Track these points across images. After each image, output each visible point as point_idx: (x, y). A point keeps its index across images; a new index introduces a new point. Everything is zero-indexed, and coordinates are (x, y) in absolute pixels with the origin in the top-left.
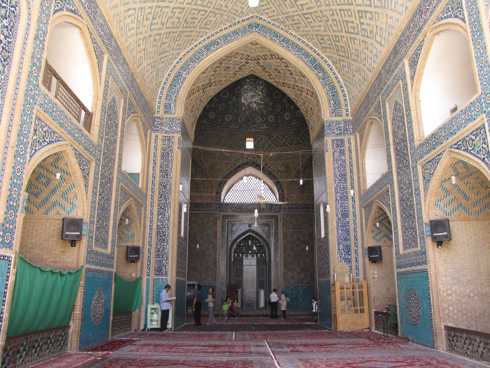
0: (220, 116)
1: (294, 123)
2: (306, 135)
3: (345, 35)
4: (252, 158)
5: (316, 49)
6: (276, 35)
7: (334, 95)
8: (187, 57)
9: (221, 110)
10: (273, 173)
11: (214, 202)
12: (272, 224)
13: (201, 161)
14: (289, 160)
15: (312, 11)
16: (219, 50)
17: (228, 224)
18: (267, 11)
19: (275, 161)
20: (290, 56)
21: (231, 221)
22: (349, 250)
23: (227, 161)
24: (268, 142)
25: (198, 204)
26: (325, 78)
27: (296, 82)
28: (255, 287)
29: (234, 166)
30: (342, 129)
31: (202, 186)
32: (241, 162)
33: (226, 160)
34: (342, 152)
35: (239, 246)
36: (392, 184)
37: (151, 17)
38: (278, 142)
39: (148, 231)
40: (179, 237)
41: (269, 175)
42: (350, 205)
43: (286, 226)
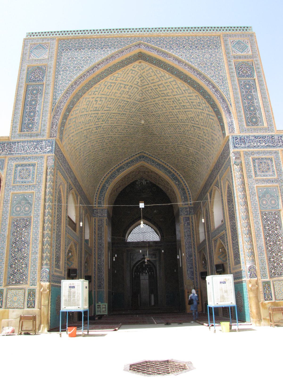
3: (187, 168)
5: (175, 169)
6: (153, 162)
7: (184, 193)
8: (108, 176)
15: (171, 154)
16: (124, 172)
18: (148, 150)
20: (161, 173)
22: (193, 273)
26: (179, 184)
27: (165, 184)
28: (148, 293)
30: (188, 211)
34: (188, 224)
35: (137, 268)
36: (206, 245)
37: (92, 167)
39: (93, 267)
40: (109, 269)
42: (193, 251)
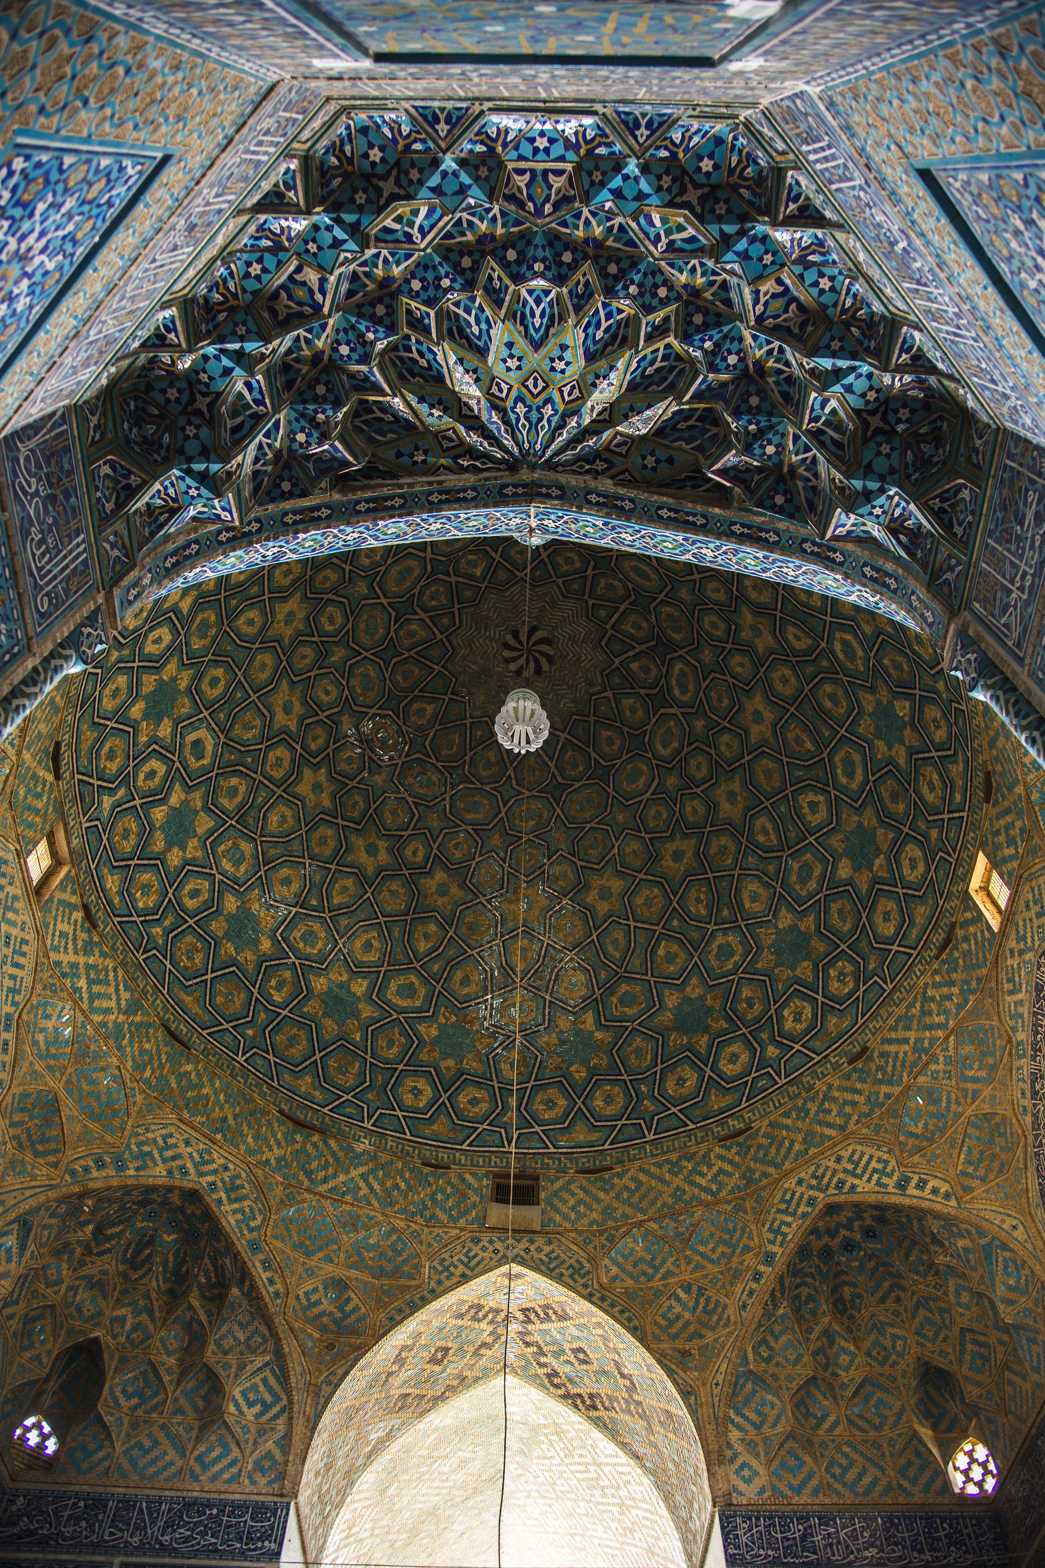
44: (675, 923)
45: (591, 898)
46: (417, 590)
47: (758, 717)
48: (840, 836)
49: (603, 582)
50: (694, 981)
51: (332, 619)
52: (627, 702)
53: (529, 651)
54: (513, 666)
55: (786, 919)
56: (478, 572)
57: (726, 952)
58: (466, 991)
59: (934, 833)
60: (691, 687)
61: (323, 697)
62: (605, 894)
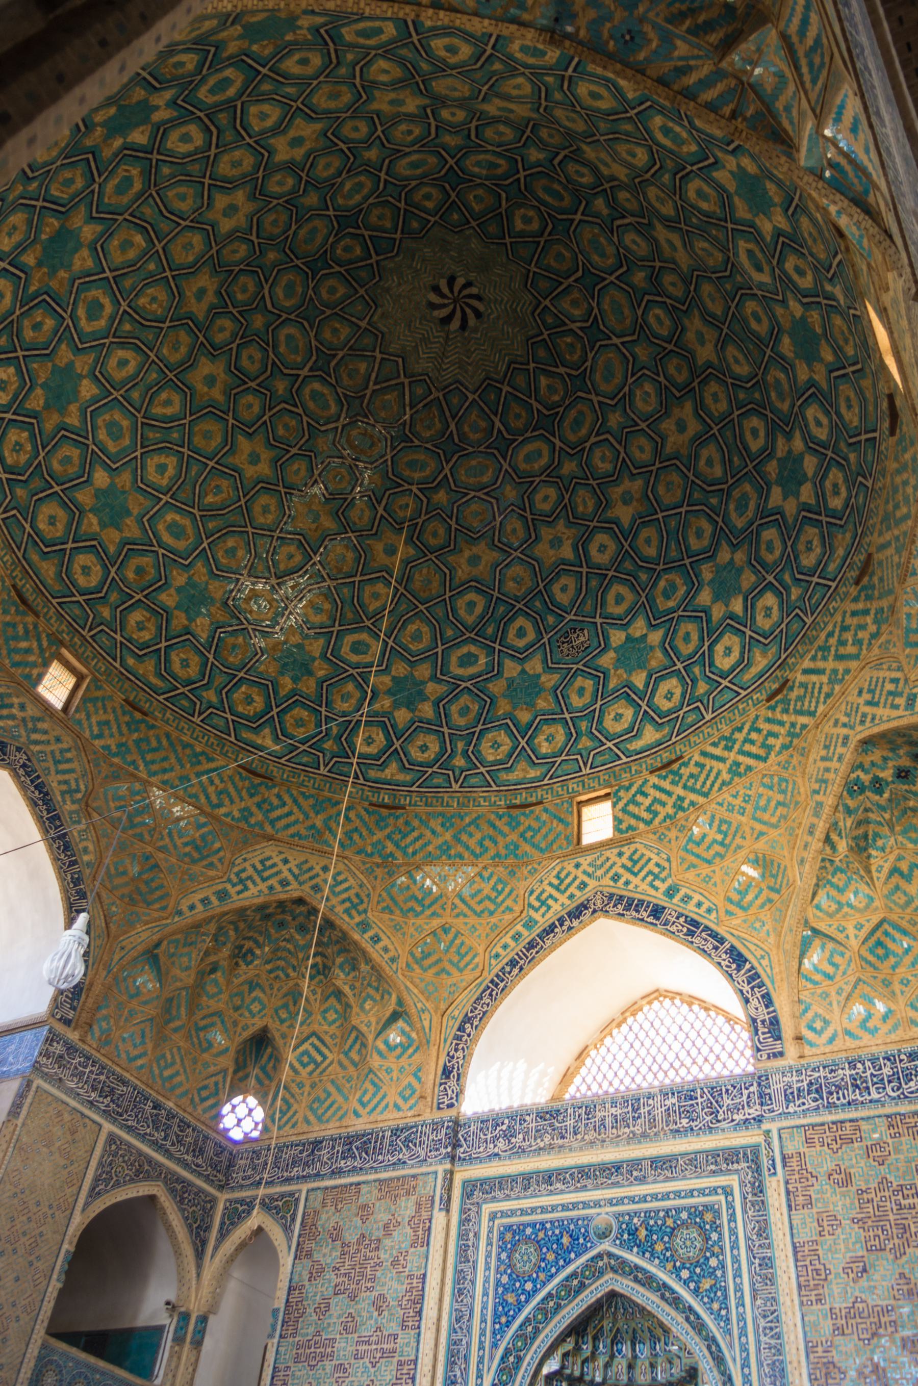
0: (460, 745)
1: (760, 662)
2: (814, 678)
4: (607, 881)
9: (462, 722)
10: (709, 921)
11: (429, 1116)
12: (730, 1206)
13: (364, 926)
14: (774, 833)
17: (490, 1231)
19: (709, 862)
21: (504, 1214)
23: (493, 920)
24: (669, 794)
25: (358, 1136)
29: (525, 933)
31: (382, 1046)
32: (556, 907)
33: (491, 913)
38: (708, 776)
41: (690, 933)
43: (810, 1203)
44: (152, 266)
45: (240, 197)
46: (590, 356)
47: (254, 459)
48: (128, 484)
49: (438, 425)
50: (90, 263)
51: (658, 320)
52: (345, 332)
53: (455, 301)
54: (461, 281)
55: (88, 389)
56: (544, 381)
57: (95, 308)
58: (297, 57)
59: (106, 613)
60: (311, 405)
61: (638, 240)
62: (232, 209)
